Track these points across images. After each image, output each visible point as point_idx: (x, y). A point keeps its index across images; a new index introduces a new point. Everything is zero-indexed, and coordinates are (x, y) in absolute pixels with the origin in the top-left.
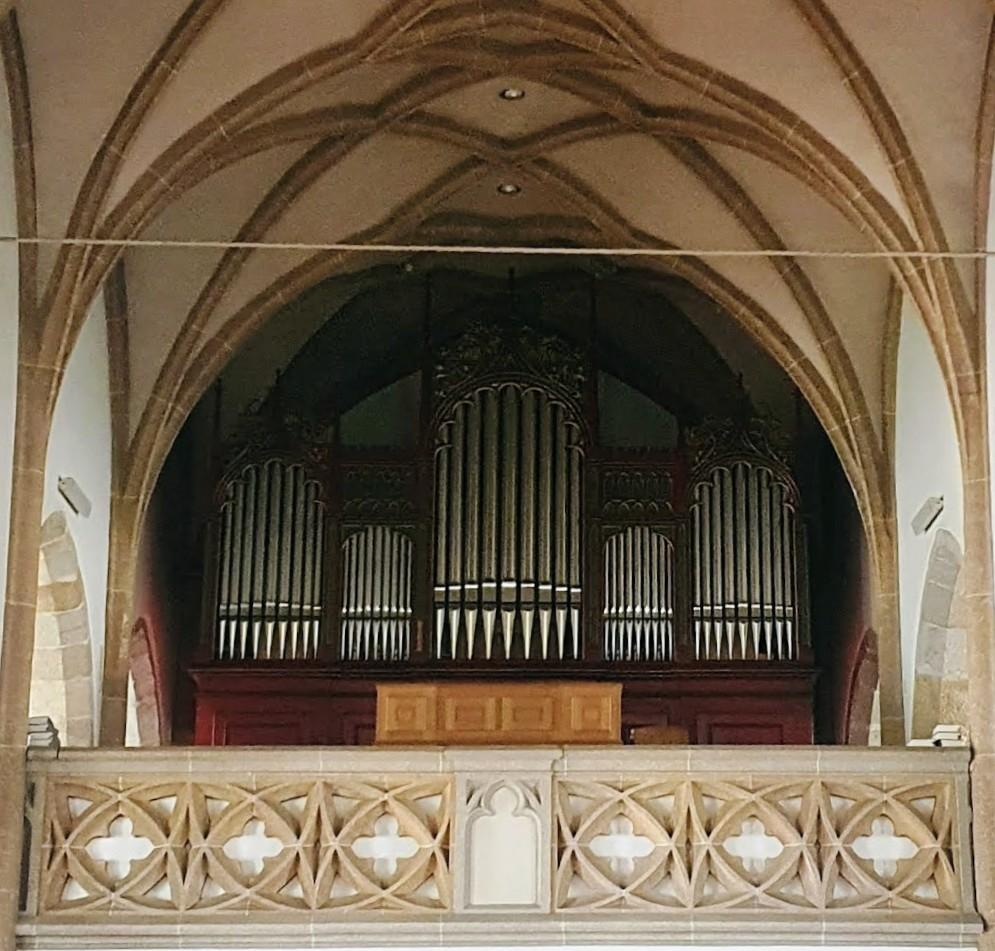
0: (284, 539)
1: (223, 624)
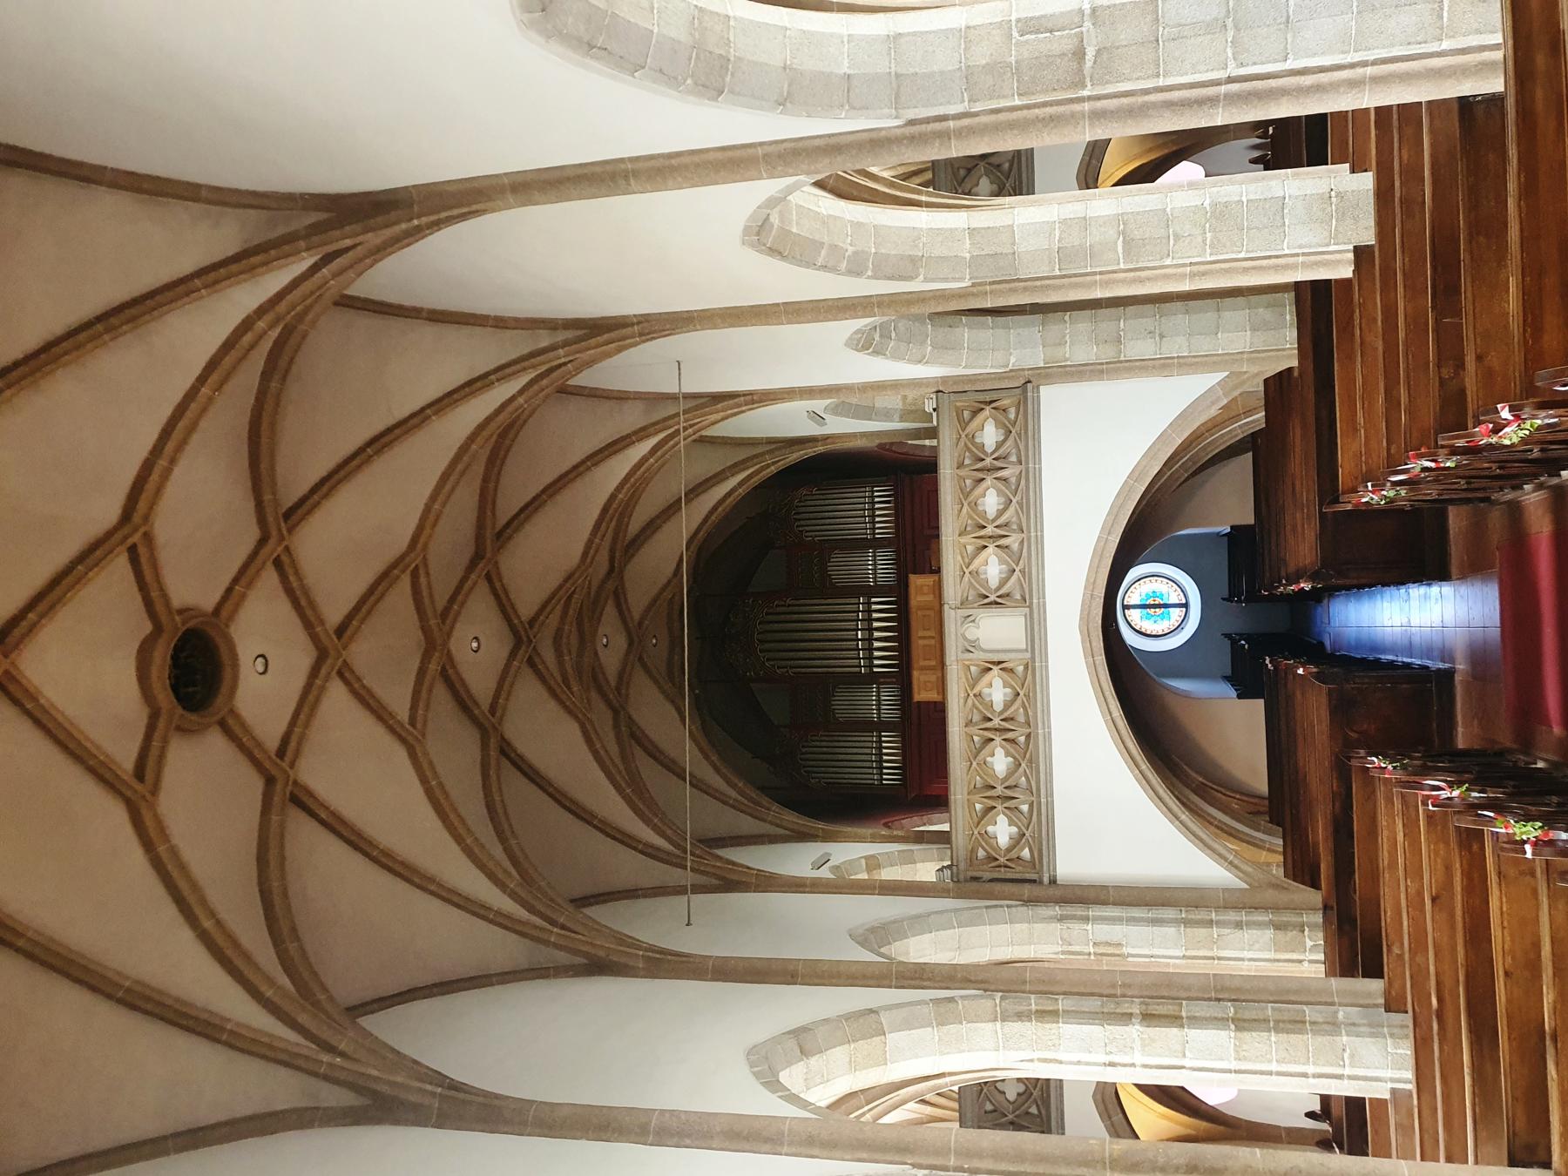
0: (806, 638)
1: (875, 670)
